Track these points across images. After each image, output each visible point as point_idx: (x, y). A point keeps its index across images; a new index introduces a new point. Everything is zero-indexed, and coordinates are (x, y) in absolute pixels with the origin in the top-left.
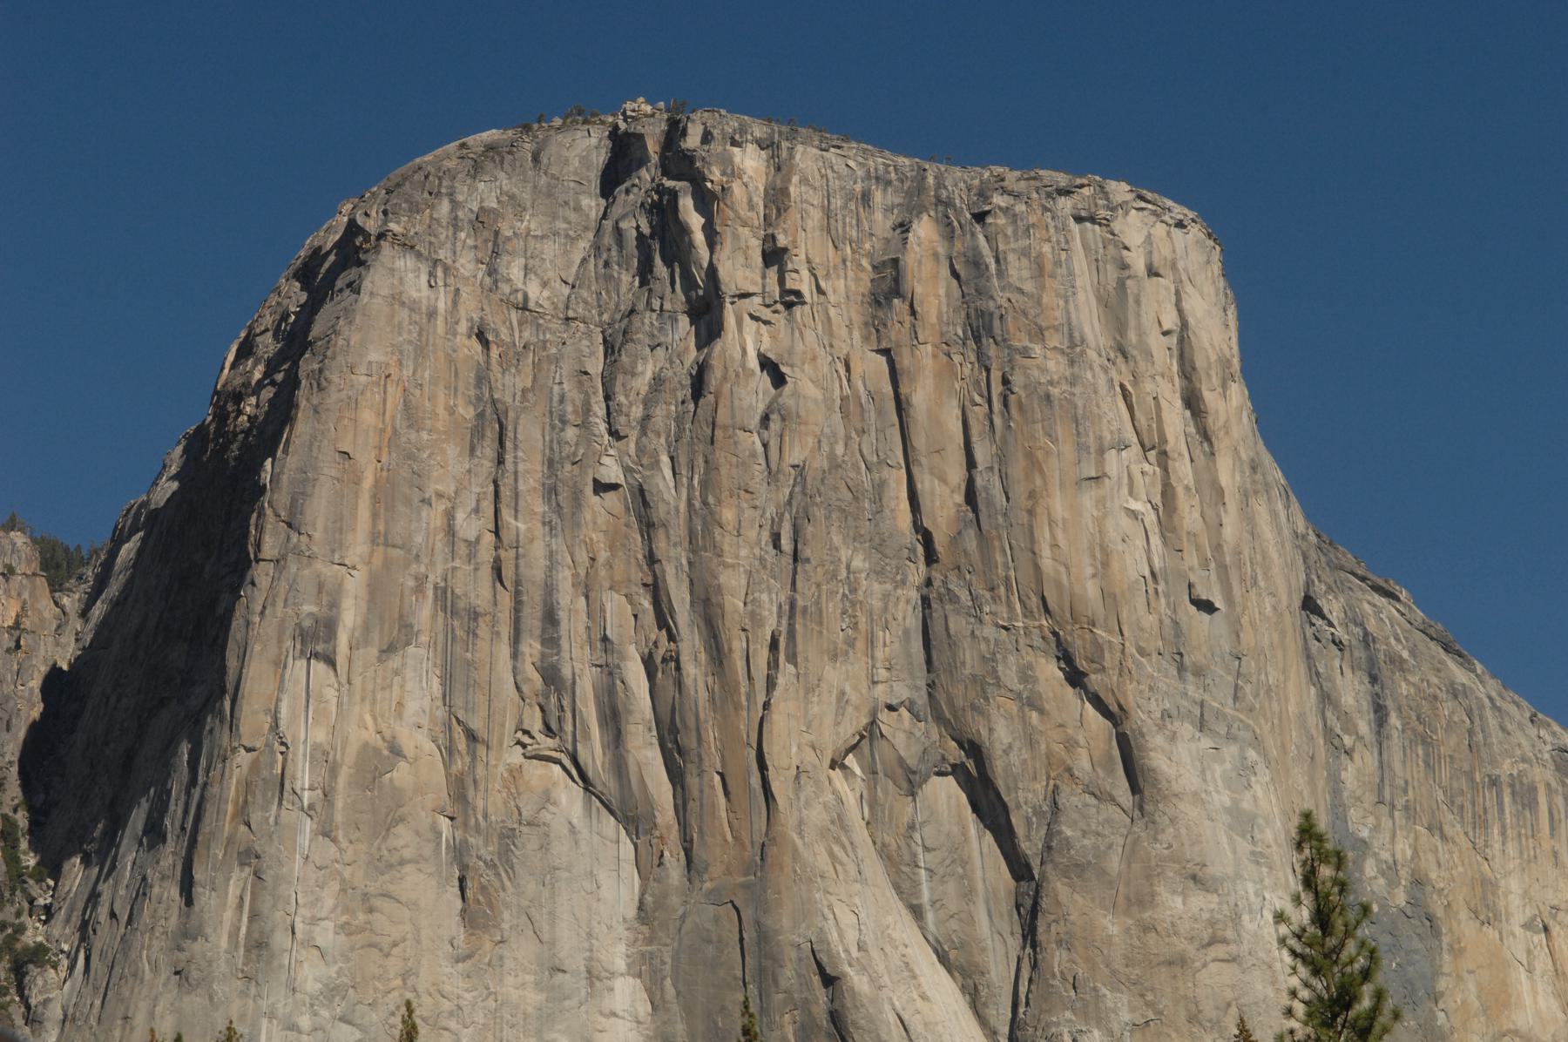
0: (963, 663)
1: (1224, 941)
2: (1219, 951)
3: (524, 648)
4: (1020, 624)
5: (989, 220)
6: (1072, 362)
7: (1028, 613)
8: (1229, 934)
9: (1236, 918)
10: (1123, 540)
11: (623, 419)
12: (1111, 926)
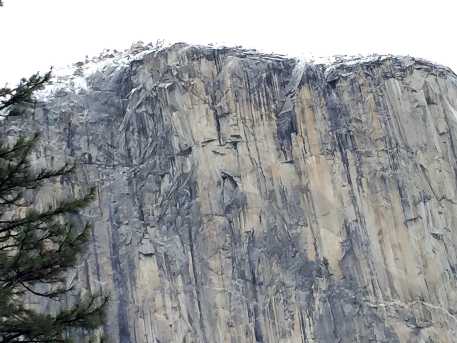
0: (355, 331)
4: (383, 305)
6: (393, 157)
7: (386, 299)
10: (434, 252)
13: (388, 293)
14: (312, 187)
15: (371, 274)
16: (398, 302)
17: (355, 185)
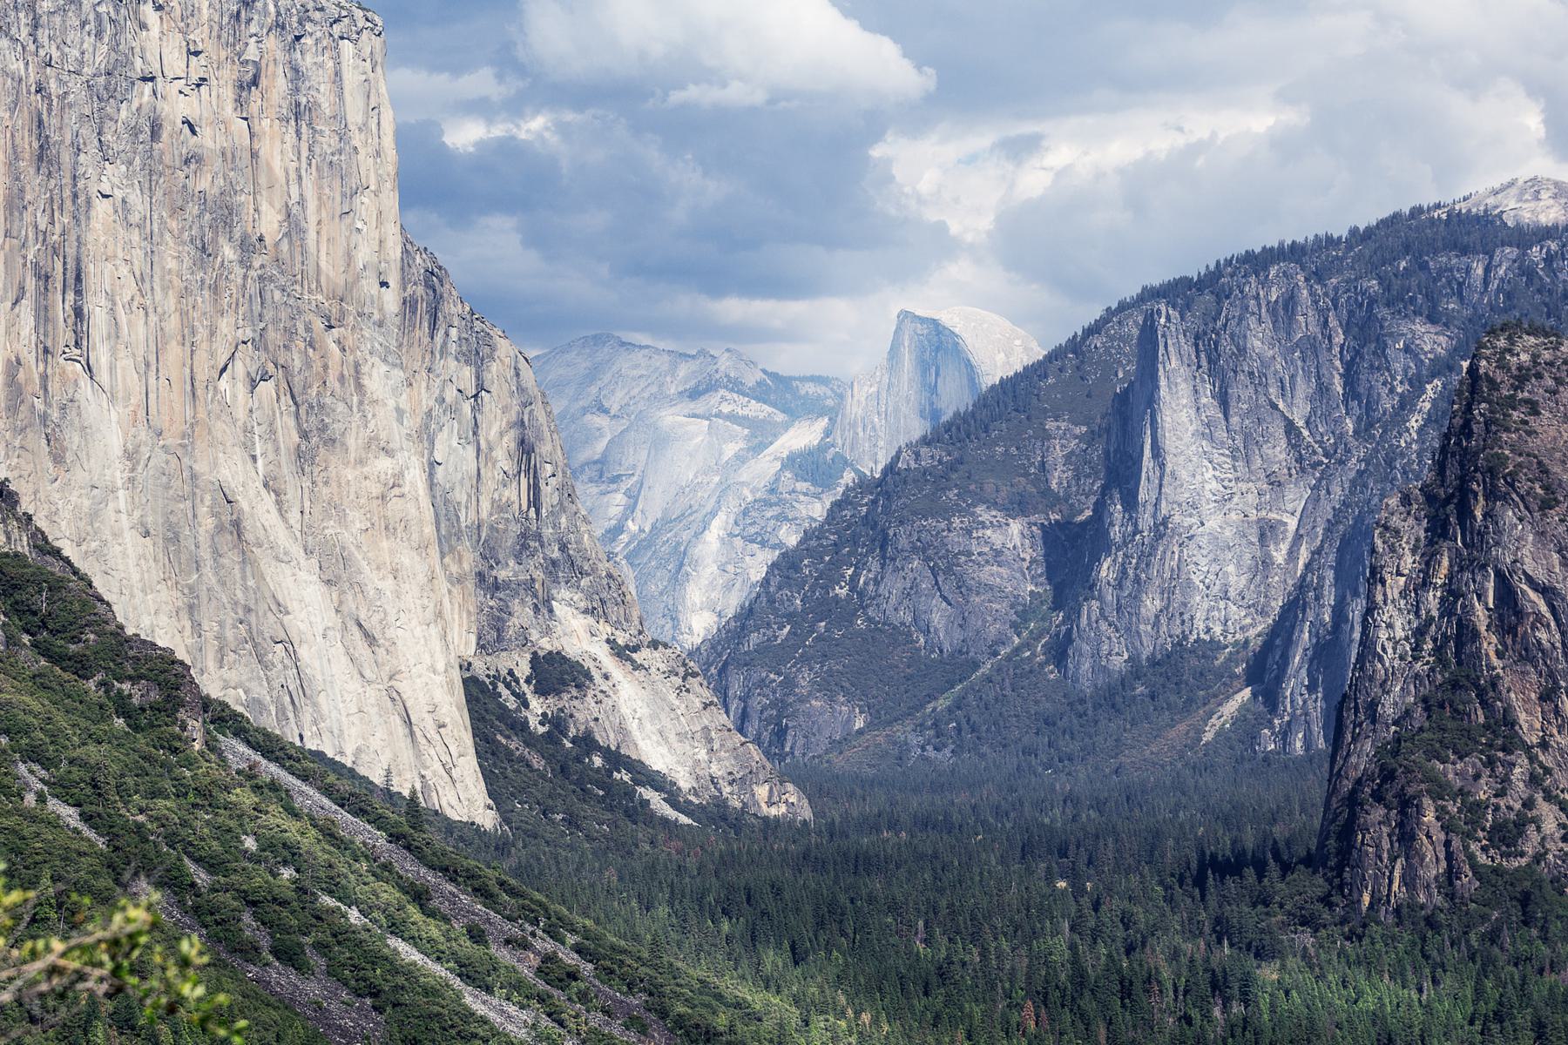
1: (399, 486)
2: (396, 491)
3: (67, 297)
5: (303, 41)
8: (401, 482)
9: (401, 474)
11: (110, 152)
12: (350, 474)
13: (314, 286)
14: (261, 153)
15: (303, 263)
16: (320, 297)
17: (304, 165)
